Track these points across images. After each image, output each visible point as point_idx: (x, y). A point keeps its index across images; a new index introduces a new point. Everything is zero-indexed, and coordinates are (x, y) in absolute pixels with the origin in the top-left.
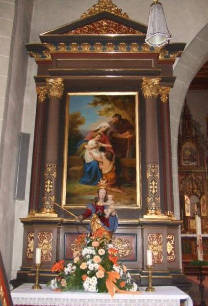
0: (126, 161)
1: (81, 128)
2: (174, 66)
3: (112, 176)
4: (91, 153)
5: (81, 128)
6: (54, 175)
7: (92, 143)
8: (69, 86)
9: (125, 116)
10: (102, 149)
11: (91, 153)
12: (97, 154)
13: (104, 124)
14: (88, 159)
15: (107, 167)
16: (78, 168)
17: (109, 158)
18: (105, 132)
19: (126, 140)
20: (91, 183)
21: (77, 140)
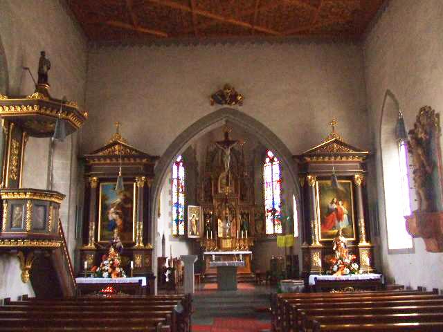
0: (128, 219)
1: (107, 202)
2: (155, 167)
3: (122, 227)
4: (112, 216)
5: (107, 202)
6: (94, 227)
7: (112, 210)
8: (100, 180)
9: (128, 194)
10: (117, 213)
11: (112, 216)
12: (114, 216)
13: (118, 200)
14: (110, 218)
15: (119, 222)
16: (106, 223)
17: (120, 217)
18: (119, 204)
19: (128, 208)
20: (110, 230)
21: (106, 208)
